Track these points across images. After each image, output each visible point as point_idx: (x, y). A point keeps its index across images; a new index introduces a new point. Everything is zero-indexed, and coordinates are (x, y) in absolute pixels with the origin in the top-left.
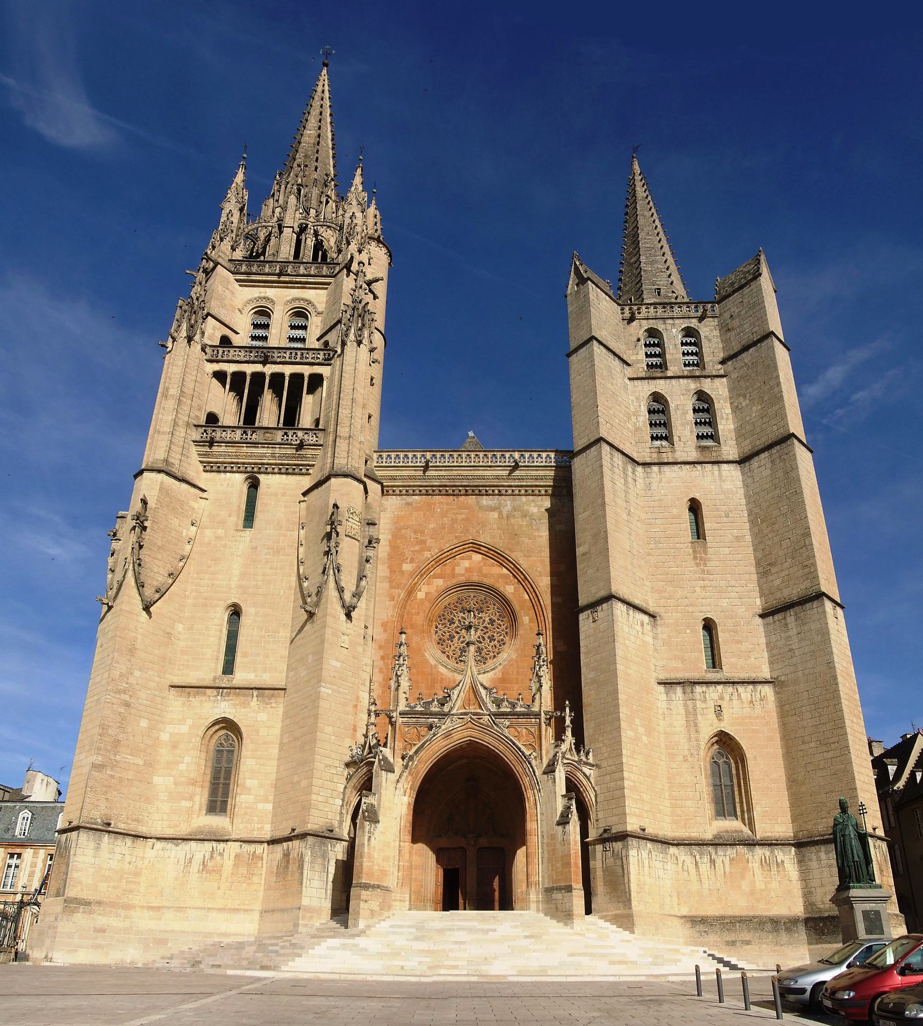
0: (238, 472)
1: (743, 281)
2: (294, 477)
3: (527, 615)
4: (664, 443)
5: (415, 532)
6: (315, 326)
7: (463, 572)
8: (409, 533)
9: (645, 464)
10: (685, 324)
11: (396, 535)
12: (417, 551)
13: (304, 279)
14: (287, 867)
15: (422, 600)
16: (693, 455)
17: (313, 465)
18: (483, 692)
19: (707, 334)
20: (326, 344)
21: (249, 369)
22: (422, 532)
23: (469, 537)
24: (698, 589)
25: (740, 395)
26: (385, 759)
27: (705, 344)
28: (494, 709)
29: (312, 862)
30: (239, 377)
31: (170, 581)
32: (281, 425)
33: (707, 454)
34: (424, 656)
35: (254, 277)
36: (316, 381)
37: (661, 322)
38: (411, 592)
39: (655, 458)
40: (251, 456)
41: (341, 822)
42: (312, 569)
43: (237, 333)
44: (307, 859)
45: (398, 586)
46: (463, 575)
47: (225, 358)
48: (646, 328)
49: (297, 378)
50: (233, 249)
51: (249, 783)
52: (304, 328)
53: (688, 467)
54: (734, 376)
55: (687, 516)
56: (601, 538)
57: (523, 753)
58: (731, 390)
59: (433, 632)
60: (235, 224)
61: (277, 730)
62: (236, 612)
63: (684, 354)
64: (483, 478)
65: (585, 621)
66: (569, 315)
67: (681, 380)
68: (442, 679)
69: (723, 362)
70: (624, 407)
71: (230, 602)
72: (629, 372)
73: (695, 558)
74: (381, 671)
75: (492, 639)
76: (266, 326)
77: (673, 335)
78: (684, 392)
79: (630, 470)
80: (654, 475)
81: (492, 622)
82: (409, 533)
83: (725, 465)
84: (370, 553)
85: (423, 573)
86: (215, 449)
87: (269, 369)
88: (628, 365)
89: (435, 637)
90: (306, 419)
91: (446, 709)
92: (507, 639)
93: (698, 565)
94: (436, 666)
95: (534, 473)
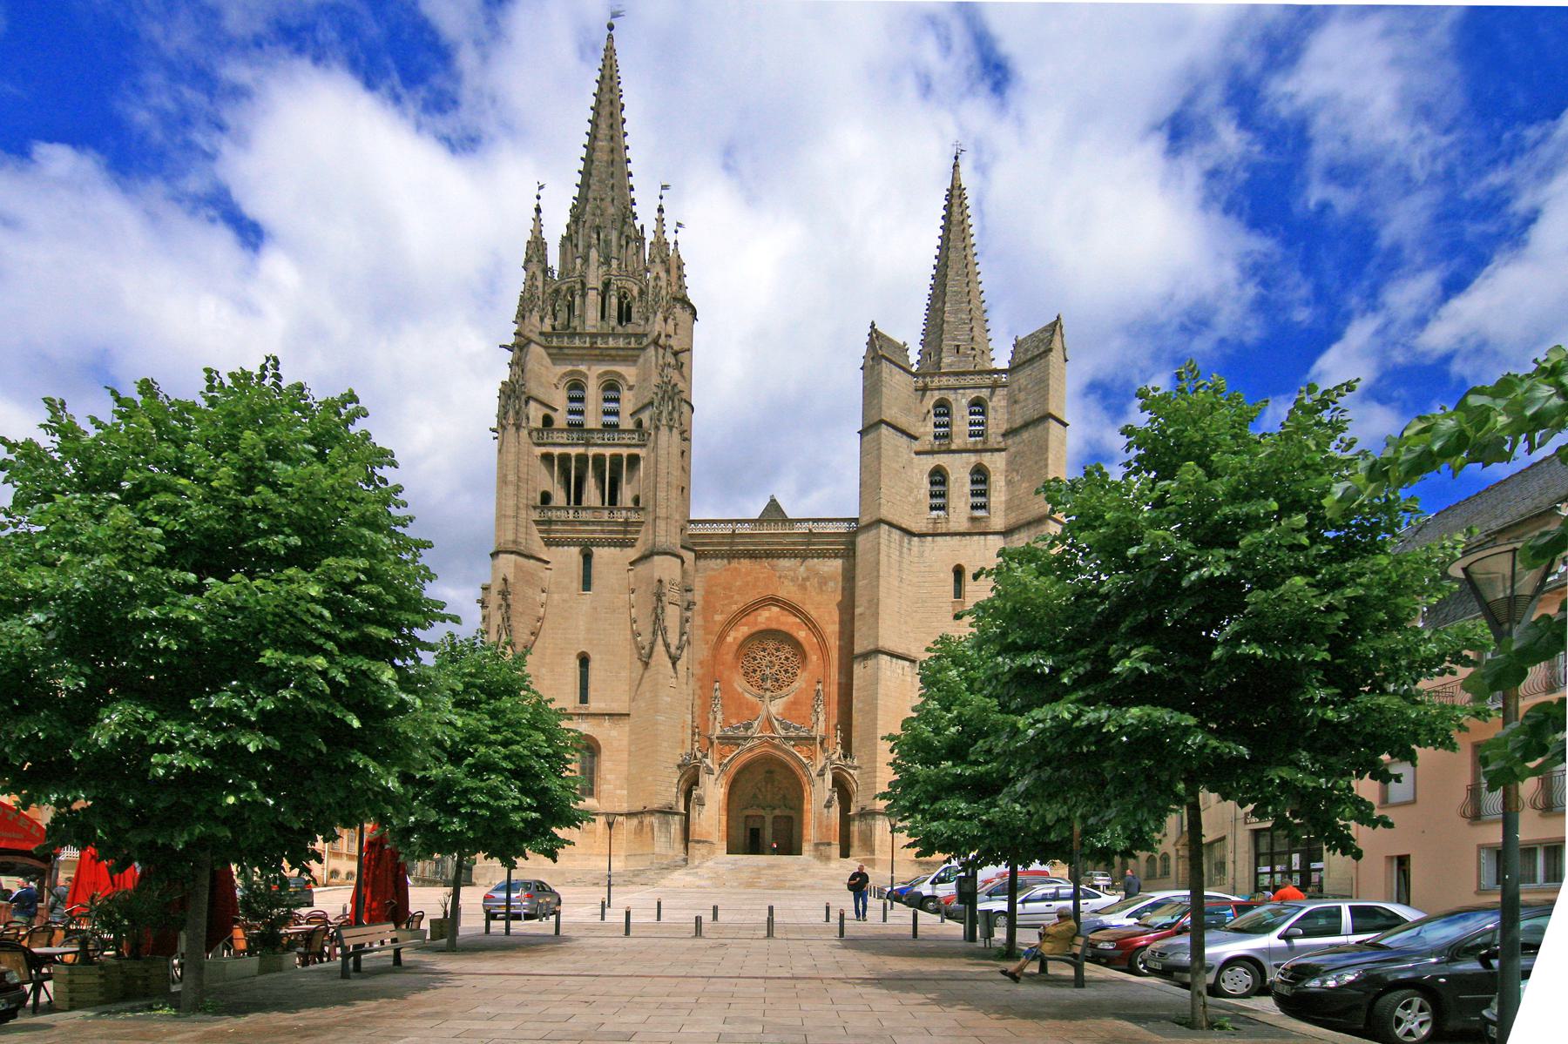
1: (1036, 353)
4: (941, 513)
5: (724, 589)
6: (628, 402)
9: (922, 535)
10: (973, 394)
11: (708, 593)
13: (613, 352)
14: (642, 829)
16: (964, 526)
18: (776, 723)
20: (639, 424)
21: (573, 451)
22: (730, 589)
23: (769, 593)
25: (1014, 470)
26: (707, 766)
27: (991, 414)
28: (783, 733)
30: (564, 459)
32: (606, 504)
33: (977, 524)
35: (566, 351)
36: (634, 460)
38: (722, 637)
39: (929, 528)
41: (677, 802)
42: (645, 627)
43: (556, 410)
45: (711, 633)
47: (550, 440)
49: (616, 459)
50: (542, 320)
51: (608, 777)
52: (617, 400)
54: (1012, 450)
55: (951, 578)
56: (875, 604)
60: (541, 289)
61: (625, 742)
63: (971, 425)
65: (858, 669)
69: (1004, 435)
76: (581, 400)
79: (906, 540)
81: (787, 659)
84: (689, 614)
85: (733, 622)
87: (592, 451)
89: (742, 671)
90: (626, 495)
91: (749, 733)
92: (799, 672)
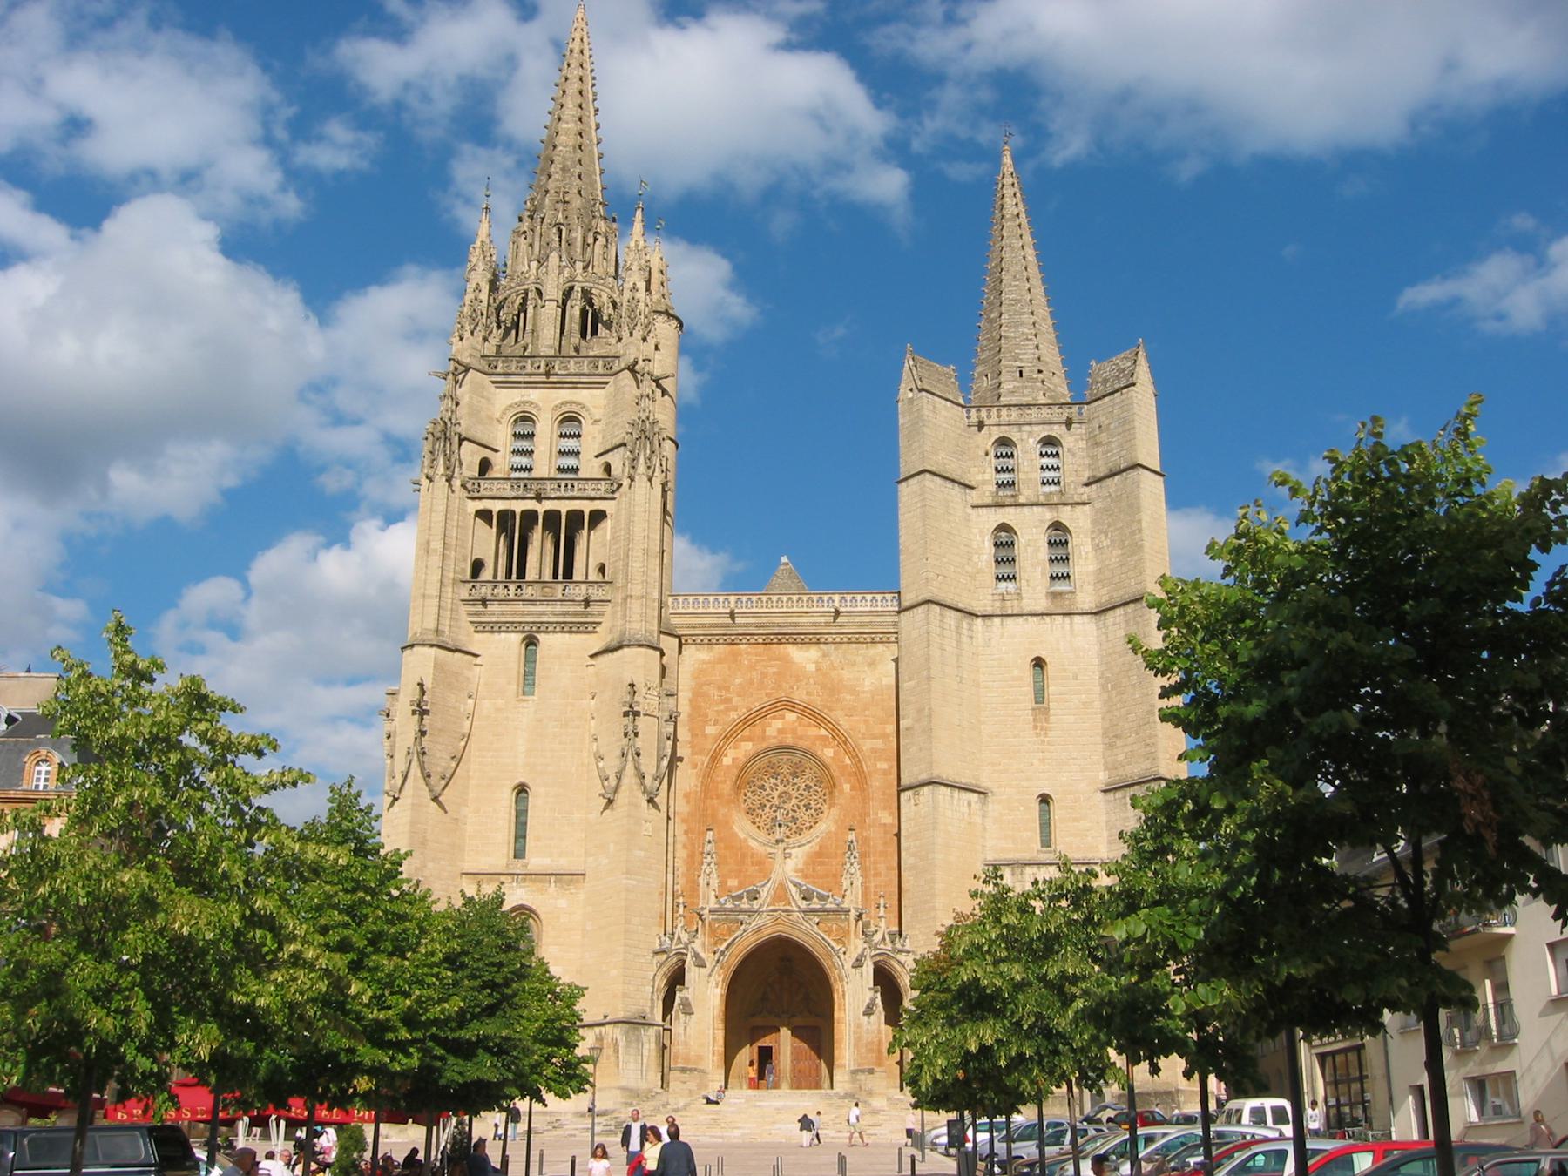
0: (513, 632)
2: (579, 636)
3: (849, 782)
5: (719, 688)
6: (592, 440)
7: (775, 734)
8: (714, 693)
10: (1044, 432)
12: (722, 711)
15: (728, 766)
16: (1042, 604)
17: (600, 623)
19: (1072, 445)
23: (782, 695)
24: (1035, 762)
29: (627, 1046)
31: (454, 764)
34: (732, 828)
37: (1015, 429)
38: (715, 758)
40: (529, 614)
44: (622, 1044)
46: (775, 737)
48: (997, 437)
53: (1035, 619)
54: (1098, 505)
57: (832, 948)
58: (1094, 522)
59: (741, 800)
62: (522, 790)
64: (796, 625)
66: (900, 428)
67: (1035, 508)
68: (753, 854)
70: (962, 547)
71: (517, 782)
72: (974, 496)
73: (1035, 727)
74: (685, 847)
75: (808, 807)
77: (1028, 445)
78: (1037, 523)
80: (995, 629)
82: (714, 693)
83: (1078, 617)
85: (729, 737)
86: (489, 608)
88: (972, 488)
92: (825, 807)
93: (1038, 735)
94: (746, 840)
95: (857, 619)
